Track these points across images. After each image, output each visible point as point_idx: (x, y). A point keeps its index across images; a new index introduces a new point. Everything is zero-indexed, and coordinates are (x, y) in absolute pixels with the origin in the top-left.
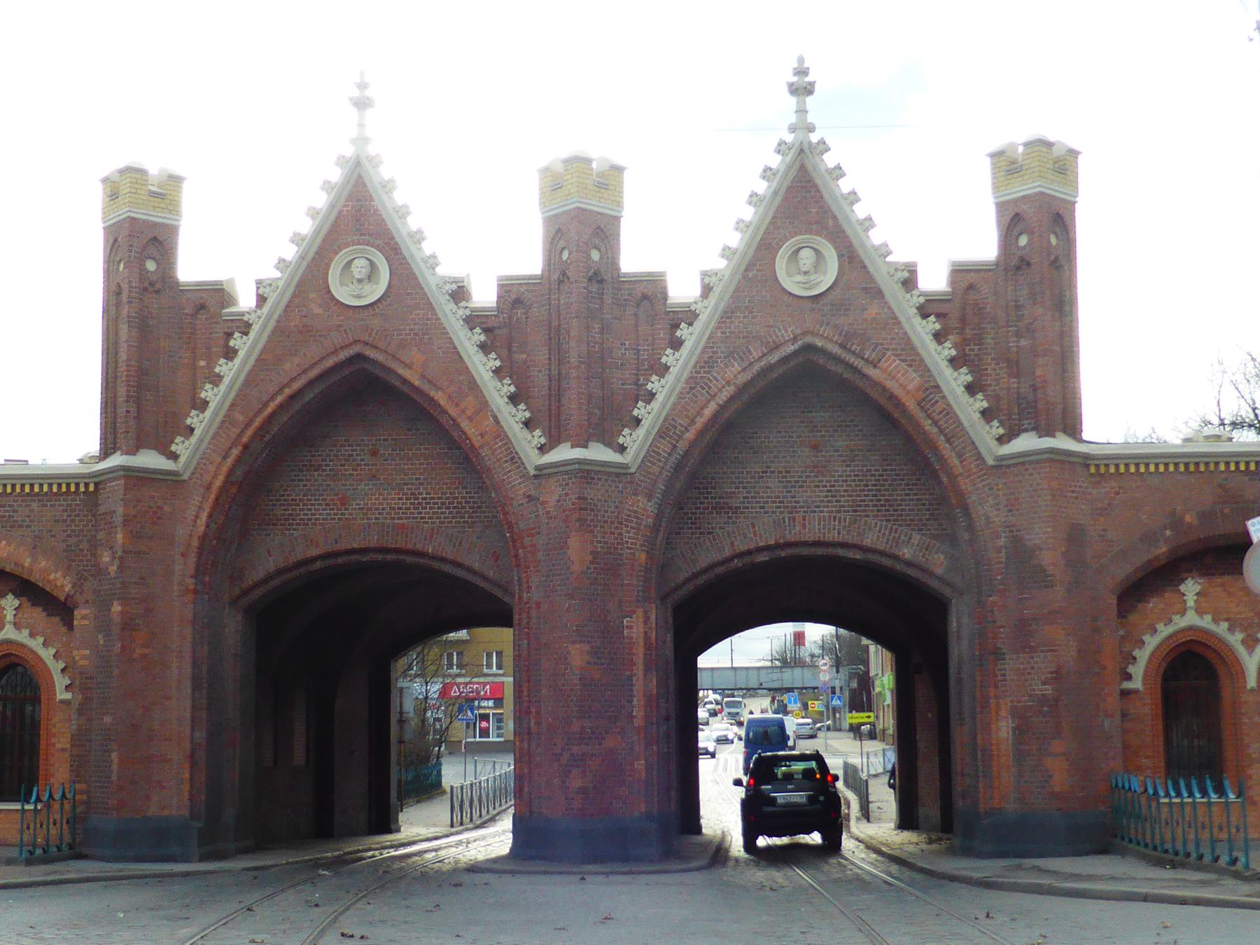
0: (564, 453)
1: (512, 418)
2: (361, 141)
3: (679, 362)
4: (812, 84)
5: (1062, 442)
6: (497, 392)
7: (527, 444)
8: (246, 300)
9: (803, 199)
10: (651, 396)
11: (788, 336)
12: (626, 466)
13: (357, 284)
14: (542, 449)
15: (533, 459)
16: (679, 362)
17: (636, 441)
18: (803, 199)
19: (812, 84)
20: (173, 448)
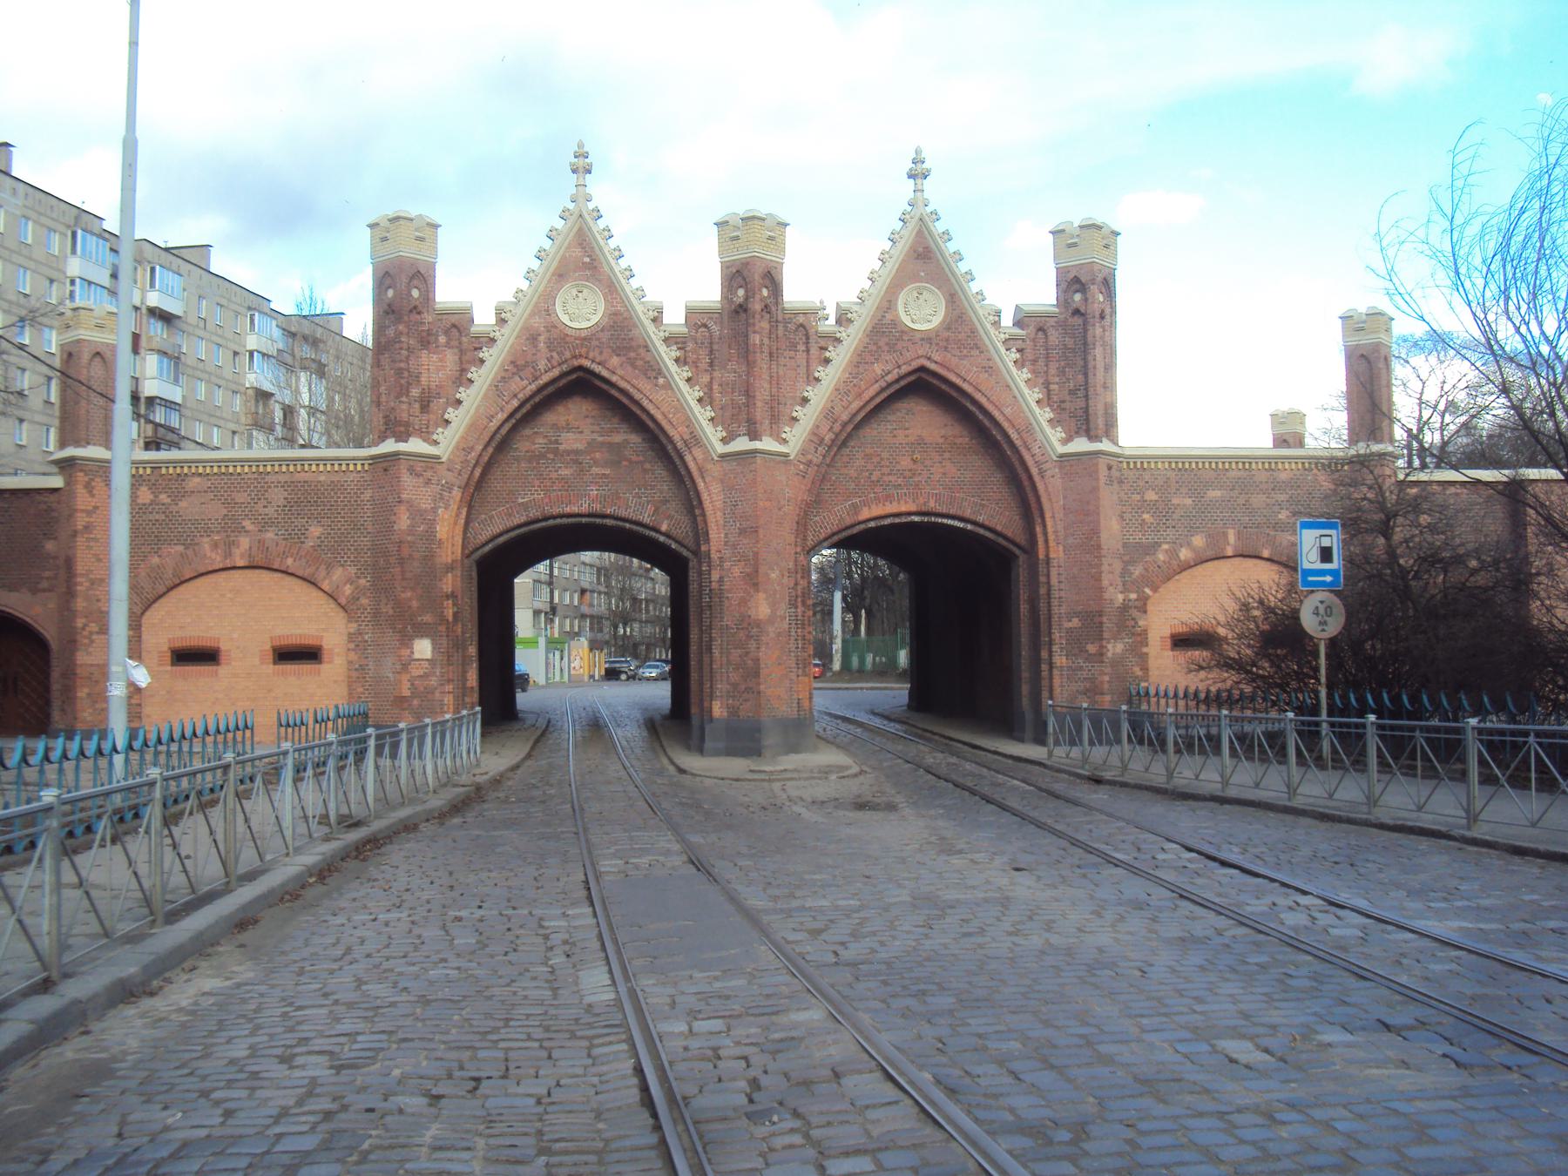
0: (742, 444)
1: (702, 415)
2: (581, 196)
3: (830, 376)
4: (929, 171)
5: (1105, 446)
6: (691, 395)
7: (713, 436)
8: (484, 318)
9: (923, 256)
10: (805, 401)
11: (910, 360)
12: (786, 455)
13: (581, 312)
14: (725, 441)
15: (721, 449)
16: (830, 376)
17: (794, 440)
18: (923, 256)
19: (929, 171)
20: (435, 437)
